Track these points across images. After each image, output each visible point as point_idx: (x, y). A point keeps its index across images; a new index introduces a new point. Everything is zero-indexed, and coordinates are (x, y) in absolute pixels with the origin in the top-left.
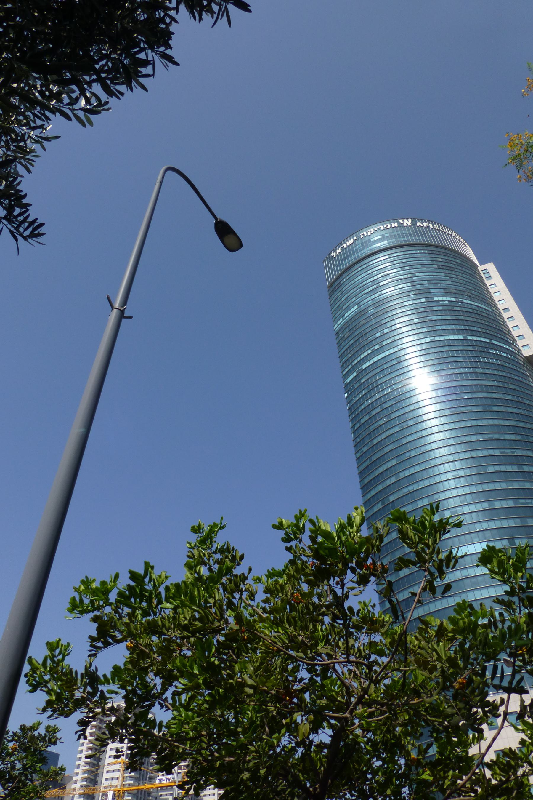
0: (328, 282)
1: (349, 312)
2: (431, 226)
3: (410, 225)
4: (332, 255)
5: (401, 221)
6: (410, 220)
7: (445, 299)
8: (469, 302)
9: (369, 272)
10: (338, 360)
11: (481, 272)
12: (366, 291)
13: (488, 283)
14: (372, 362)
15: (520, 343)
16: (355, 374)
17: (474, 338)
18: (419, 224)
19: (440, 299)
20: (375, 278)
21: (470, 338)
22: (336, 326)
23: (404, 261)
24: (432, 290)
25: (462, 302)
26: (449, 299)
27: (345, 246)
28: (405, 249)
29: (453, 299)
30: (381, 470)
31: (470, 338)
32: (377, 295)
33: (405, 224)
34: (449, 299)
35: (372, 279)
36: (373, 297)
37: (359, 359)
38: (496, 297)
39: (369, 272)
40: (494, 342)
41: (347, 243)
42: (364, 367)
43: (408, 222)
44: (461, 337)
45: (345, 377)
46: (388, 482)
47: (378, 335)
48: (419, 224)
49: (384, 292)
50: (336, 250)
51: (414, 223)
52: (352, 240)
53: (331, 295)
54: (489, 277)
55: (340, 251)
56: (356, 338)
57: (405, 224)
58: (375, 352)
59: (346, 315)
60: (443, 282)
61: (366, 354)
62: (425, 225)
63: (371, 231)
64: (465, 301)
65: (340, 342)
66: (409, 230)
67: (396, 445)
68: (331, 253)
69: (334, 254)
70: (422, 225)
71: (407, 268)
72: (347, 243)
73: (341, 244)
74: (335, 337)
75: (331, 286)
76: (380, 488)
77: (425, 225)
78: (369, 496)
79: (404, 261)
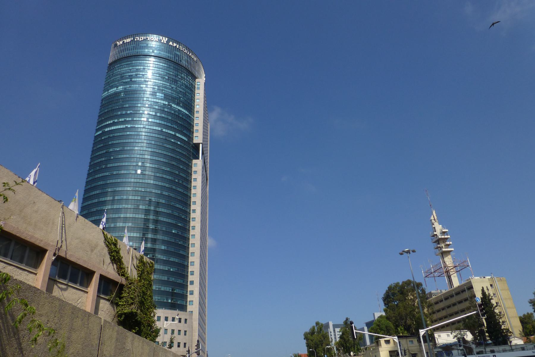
0: (110, 60)
1: (111, 90)
5: (161, 37)
6: (167, 39)
7: (162, 102)
8: (175, 106)
9: (131, 68)
10: (97, 117)
12: (124, 81)
13: (196, 91)
14: (111, 129)
15: (195, 134)
16: (101, 132)
17: (167, 131)
18: (171, 43)
19: (160, 101)
20: (132, 74)
21: (164, 130)
24: (158, 94)
25: (171, 106)
26: (164, 102)
29: (167, 103)
30: (93, 193)
31: (164, 130)
32: (128, 86)
33: (162, 41)
34: (164, 102)
35: (130, 74)
36: (126, 86)
37: (106, 124)
38: (197, 101)
39: (131, 68)
40: (177, 135)
42: (106, 130)
43: (165, 40)
44: (160, 129)
45: (97, 130)
46: (94, 201)
47: (119, 113)
48: (171, 43)
49: (132, 86)
51: (168, 42)
54: (199, 88)
56: (109, 109)
57: (162, 41)
58: (114, 124)
59: (110, 91)
60: (166, 90)
61: (110, 122)
62: (175, 45)
64: (173, 105)
65: (102, 106)
67: (104, 183)
69: (118, 43)
74: (100, 102)
75: (111, 64)
76: (90, 202)
77: (175, 45)
78: (86, 204)
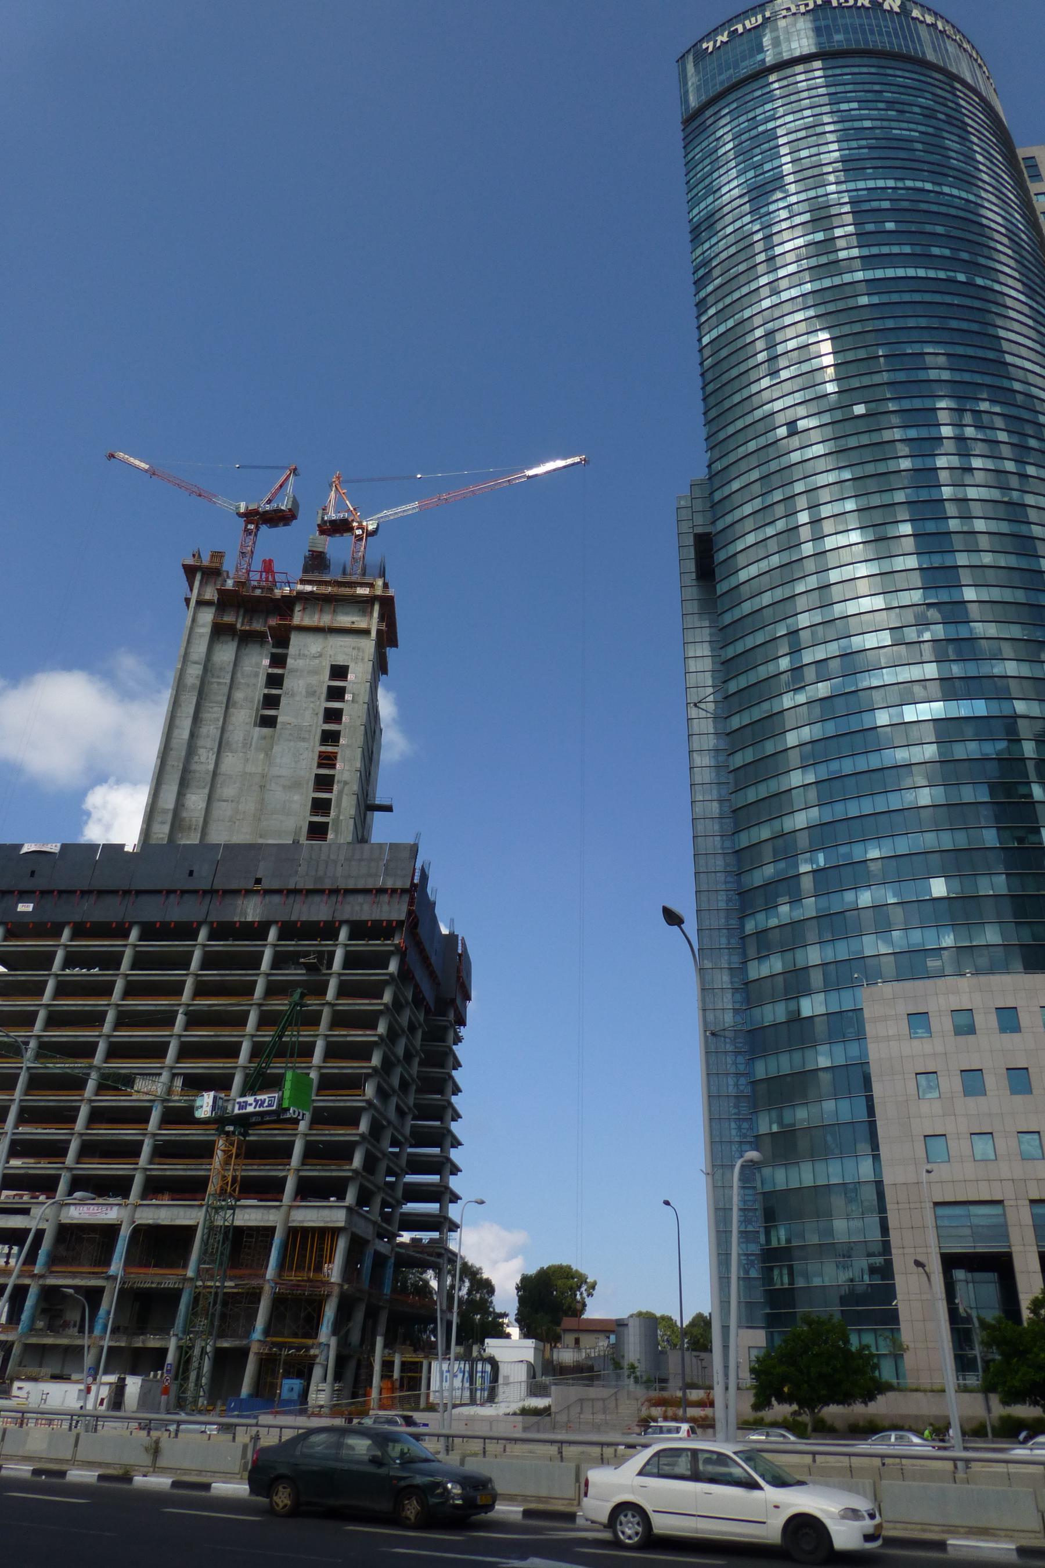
2: (940, 26)
3: (898, 10)
4: (705, 46)
11: (1021, 161)
22: (695, 211)
23: (877, 87)
27: (740, 28)
28: (884, 62)
41: (747, 23)
50: (717, 35)
52: (760, 18)
53: (688, 142)
55: (725, 39)
63: (807, 5)
66: (893, 21)
68: (701, 41)
70: (921, 18)
71: (881, 105)
72: (747, 23)
73: (730, 21)
79: (877, 87)
